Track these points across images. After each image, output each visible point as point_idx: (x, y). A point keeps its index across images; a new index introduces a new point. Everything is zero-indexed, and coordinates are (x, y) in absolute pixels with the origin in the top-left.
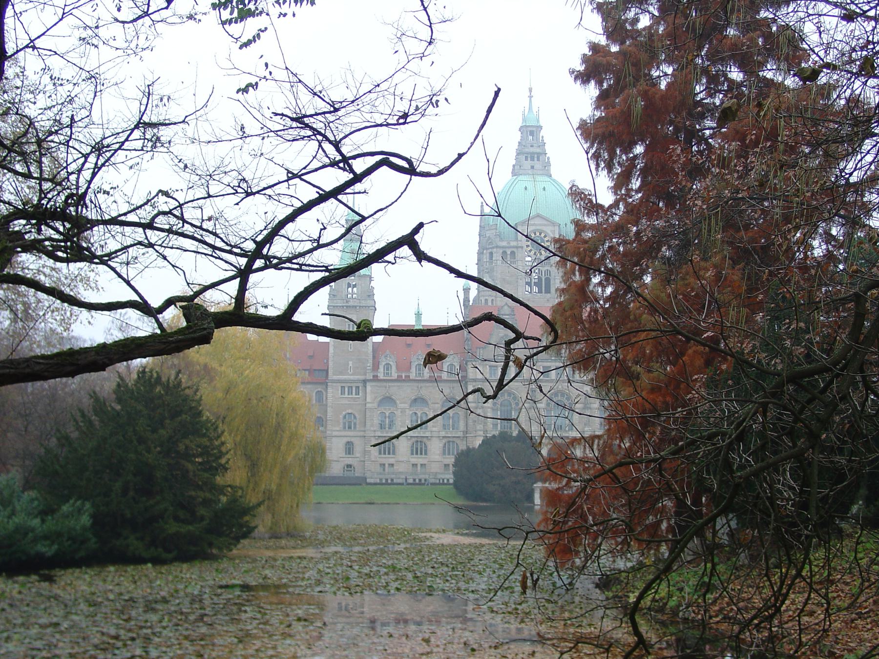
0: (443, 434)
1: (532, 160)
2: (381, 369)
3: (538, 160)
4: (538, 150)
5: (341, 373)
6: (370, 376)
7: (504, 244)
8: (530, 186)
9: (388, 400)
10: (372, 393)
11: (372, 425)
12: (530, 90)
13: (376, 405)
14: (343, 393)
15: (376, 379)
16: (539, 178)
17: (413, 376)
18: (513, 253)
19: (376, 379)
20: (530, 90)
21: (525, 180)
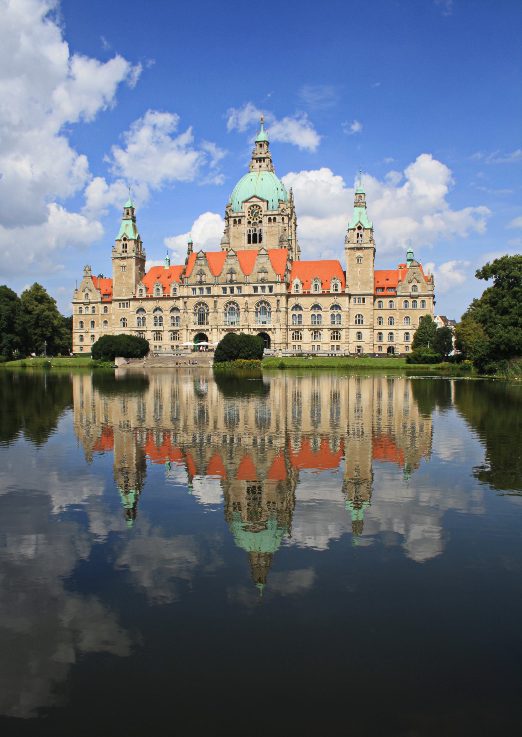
0: (170, 329)
1: (260, 161)
3: (264, 161)
4: (263, 156)
5: (119, 296)
6: (131, 297)
7: (235, 215)
9: (141, 310)
11: (133, 324)
13: (135, 313)
14: (120, 307)
15: (135, 299)
16: (262, 173)
17: (154, 296)
18: (240, 221)
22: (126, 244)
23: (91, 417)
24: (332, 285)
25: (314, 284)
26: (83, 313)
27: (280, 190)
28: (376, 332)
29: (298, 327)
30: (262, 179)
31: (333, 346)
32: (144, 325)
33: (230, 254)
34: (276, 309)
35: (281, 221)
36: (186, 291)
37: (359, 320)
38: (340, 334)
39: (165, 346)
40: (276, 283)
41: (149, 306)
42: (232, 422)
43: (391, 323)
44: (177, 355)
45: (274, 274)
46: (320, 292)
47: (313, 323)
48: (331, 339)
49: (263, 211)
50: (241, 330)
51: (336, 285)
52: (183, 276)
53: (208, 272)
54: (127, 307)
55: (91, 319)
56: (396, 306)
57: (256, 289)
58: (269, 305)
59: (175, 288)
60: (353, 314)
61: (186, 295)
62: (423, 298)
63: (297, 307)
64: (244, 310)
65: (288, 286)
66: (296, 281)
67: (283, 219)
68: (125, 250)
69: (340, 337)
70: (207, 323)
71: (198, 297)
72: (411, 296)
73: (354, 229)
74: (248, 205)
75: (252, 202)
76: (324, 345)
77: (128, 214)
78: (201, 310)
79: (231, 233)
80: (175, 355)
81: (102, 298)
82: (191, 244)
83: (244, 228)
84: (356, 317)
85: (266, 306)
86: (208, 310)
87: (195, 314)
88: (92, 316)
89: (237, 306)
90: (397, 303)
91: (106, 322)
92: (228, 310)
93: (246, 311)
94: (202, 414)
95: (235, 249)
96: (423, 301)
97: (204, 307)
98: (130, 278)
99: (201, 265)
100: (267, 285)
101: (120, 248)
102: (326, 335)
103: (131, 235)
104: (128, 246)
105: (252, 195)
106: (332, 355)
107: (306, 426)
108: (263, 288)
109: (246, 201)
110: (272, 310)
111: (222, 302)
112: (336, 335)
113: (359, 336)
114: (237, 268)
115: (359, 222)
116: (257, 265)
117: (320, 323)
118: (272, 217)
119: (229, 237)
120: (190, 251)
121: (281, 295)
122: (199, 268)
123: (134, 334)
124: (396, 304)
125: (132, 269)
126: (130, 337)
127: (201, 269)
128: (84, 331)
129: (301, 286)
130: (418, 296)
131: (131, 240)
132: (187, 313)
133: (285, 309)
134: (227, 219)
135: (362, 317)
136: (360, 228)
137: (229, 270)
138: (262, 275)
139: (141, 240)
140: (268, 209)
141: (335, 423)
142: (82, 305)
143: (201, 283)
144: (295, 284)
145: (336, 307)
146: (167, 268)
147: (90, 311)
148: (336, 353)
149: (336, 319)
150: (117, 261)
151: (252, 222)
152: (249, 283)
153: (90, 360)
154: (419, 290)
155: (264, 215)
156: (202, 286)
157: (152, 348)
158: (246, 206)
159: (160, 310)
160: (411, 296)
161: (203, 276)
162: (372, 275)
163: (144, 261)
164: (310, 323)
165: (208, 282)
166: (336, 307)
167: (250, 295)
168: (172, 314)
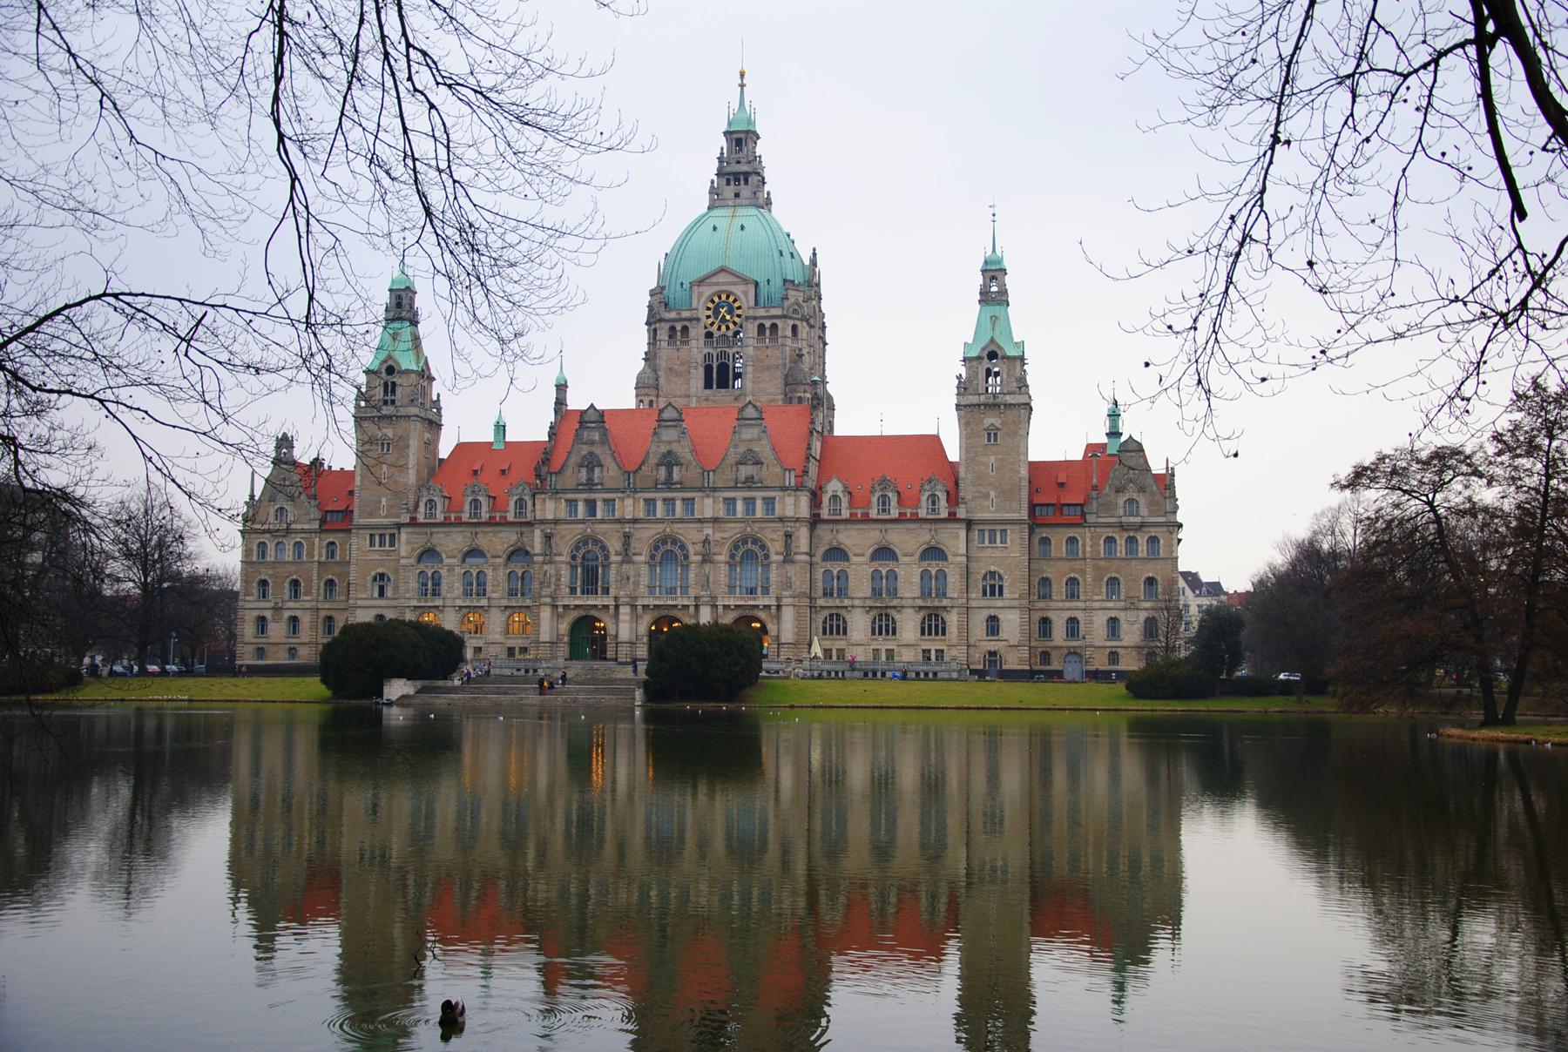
0: (505, 602)
1: (737, 180)
2: (422, 509)
3: (746, 182)
4: (745, 168)
5: (370, 515)
6: (405, 519)
7: (673, 315)
8: (722, 224)
9: (429, 553)
10: (406, 543)
11: (407, 591)
12: (742, 75)
13: (412, 561)
15: (413, 523)
16: (741, 211)
17: (465, 517)
18: (685, 329)
19: (413, 523)
20: (742, 75)
21: (721, 217)
22: (394, 384)
23: (278, 835)
24: (924, 498)
25: (878, 494)
26: (270, 557)
27: (787, 255)
28: (1037, 616)
29: (838, 602)
30: (742, 228)
31: (926, 652)
32: (436, 593)
33: (666, 415)
34: (781, 558)
35: (789, 333)
36: (549, 508)
37: (992, 587)
38: (944, 622)
39: (493, 650)
40: (783, 489)
41: (451, 543)
42: (664, 849)
43: (1073, 596)
44: (527, 671)
45: (778, 469)
46: (895, 513)
47: (876, 592)
48: (923, 633)
49: (745, 306)
50: (692, 609)
51: (933, 499)
52: (544, 469)
53: (608, 461)
54: (392, 544)
55: (291, 574)
56: (1084, 552)
57: (730, 502)
58: (763, 547)
59: (521, 500)
60: (980, 569)
61: (550, 516)
62: (1153, 532)
63: (837, 553)
64: (699, 558)
65: (815, 498)
66: (834, 486)
67: (794, 328)
68: (389, 398)
69: (944, 630)
70: (606, 591)
71: (583, 522)
72: (1122, 527)
73: (979, 358)
74: (708, 291)
75: (717, 284)
76: (904, 651)
77: (399, 305)
78: (590, 556)
79: (662, 363)
80: (522, 672)
81: (323, 521)
82: (561, 388)
83: (697, 348)
84: (984, 578)
85: (756, 548)
86: (607, 557)
87: (574, 568)
88: (293, 569)
89: (683, 547)
90: (1088, 542)
91: (330, 583)
92: (658, 559)
93: (707, 559)
94: (585, 829)
95: (679, 402)
96: (1153, 540)
97: (597, 549)
98: (404, 467)
99: (592, 443)
100: (759, 494)
101: (379, 393)
102: (909, 625)
103: (407, 362)
104: (399, 390)
105: (715, 266)
106: (926, 674)
107: (857, 859)
108: (750, 502)
109: (701, 282)
110: (774, 558)
111: (645, 537)
112: (933, 623)
113: (993, 625)
114: (684, 451)
115: (992, 341)
116: (736, 446)
117: (893, 593)
118: (768, 324)
119: (655, 371)
120: (560, 403)
121: (797, 520)
122: (585, 450)
123: (409, 616)
124: (1084, 546)
125: (408, 446)
126: (398, 624)
127: (591, 453)
128: (268, 605)
129: (845, 501)
130: (1141, 526)
131: (408, 372)
132: (551, 562)
133: (806, 558)
134: (653, 321)
135: (1001, 578)
136: (992, 355)
137: (665, 456)
138: (745, 471)
139: (434, 373)
140: (756, 303)
141: (933, 850)
142: (265, 538)
143: (590, 485)
144: (830, 494)
145: (933, 552)
146: (499, 446)
147: (289, 555)
148: (937, 668)
149: (933, 585)
150: (365, 424)
151: (717, 334)
152: (715, 489)
153: (314, 687)
154: (1144, 511)
155: (747, 318)
156: (593, 496)
157: (469, 654)
158: (700, 295)
159: (481, 554)
160: (1122, 527)
161: (597, 470)
162: (1024, 472)
163: (439, 426)
164: (869, 594)
165: (609, 484)
166: (933, 552)
167: (715, 520)
168: (512, 566)
